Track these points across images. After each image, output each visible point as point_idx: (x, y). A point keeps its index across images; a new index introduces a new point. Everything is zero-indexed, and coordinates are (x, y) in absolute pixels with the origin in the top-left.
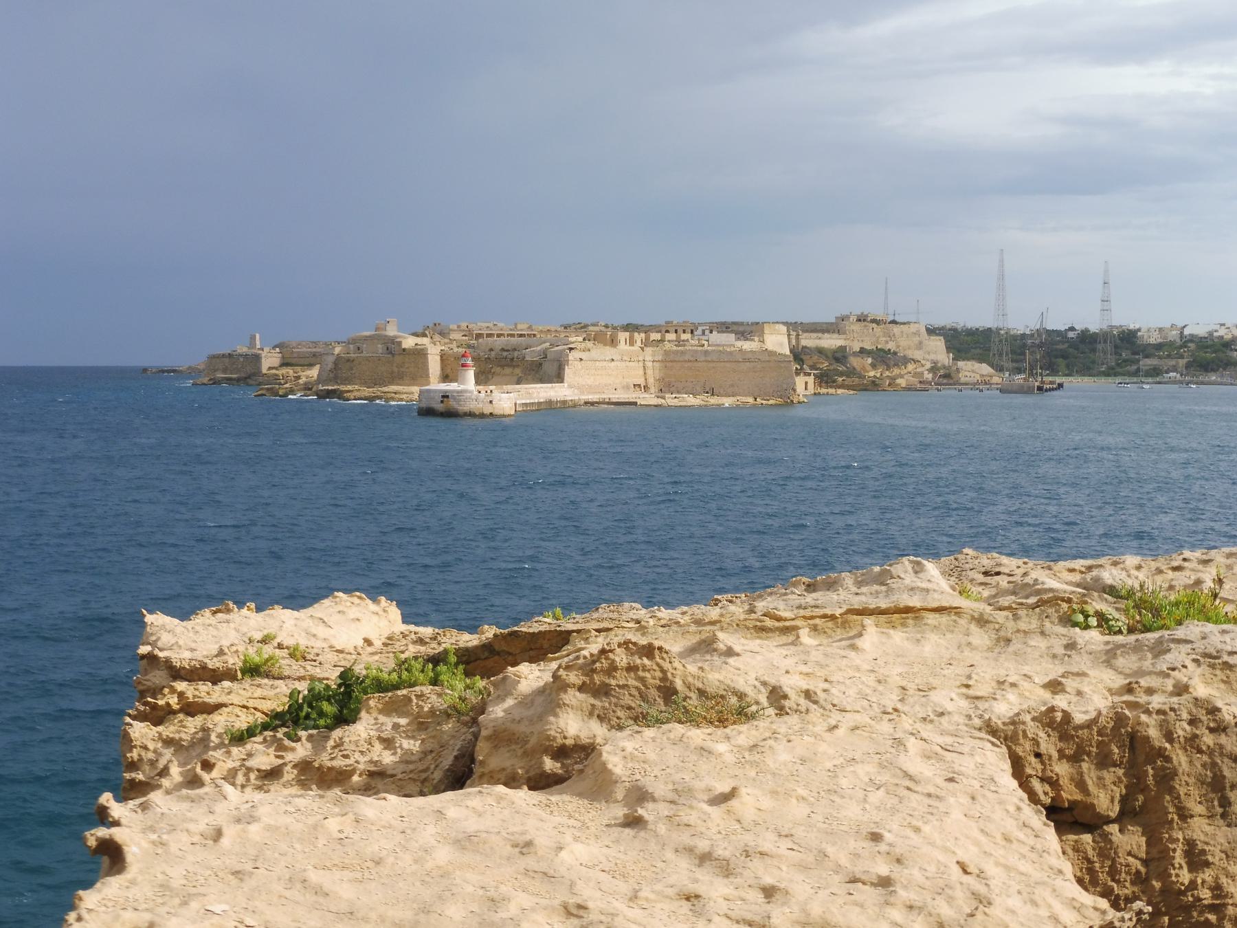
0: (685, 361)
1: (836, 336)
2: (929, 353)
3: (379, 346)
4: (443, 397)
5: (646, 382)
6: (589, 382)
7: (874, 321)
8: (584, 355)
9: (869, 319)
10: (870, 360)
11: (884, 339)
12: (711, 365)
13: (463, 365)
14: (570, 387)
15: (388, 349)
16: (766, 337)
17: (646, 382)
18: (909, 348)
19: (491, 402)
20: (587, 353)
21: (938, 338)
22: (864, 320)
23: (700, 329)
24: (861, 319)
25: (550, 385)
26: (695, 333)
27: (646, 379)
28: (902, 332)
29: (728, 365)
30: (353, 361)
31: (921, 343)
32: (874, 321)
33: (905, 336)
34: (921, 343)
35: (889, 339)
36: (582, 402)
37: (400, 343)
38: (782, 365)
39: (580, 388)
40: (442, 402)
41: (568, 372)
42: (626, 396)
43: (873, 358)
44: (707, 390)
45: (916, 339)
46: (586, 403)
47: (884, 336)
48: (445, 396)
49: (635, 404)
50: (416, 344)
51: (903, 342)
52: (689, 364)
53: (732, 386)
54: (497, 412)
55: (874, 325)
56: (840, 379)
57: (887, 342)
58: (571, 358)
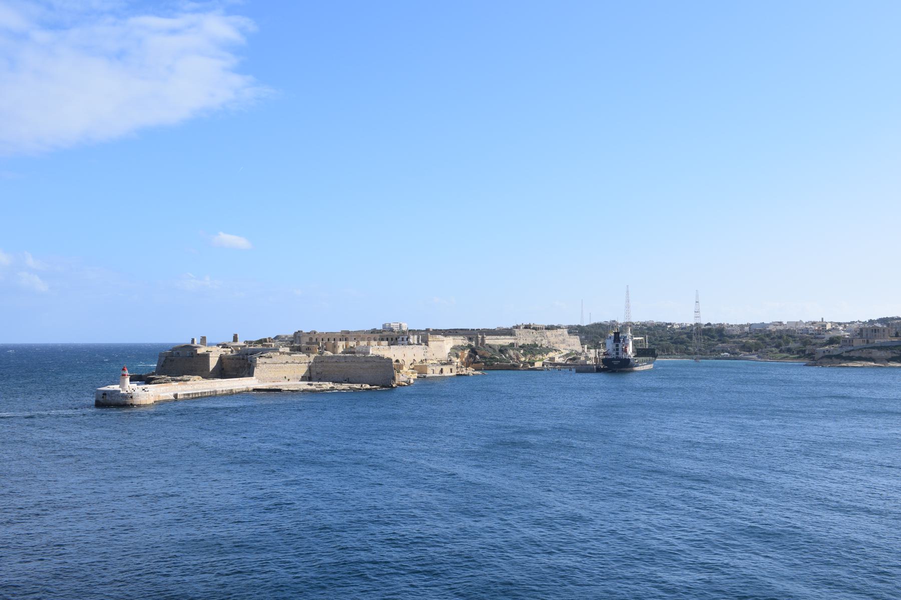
0: (333, 362)
1: (508, 337)
2: (569, 345)
4: (103, 394)
5: (310, 375)
6: (271, 376)
7: (534, 328)
8: (268, 361)
10: (522, 351)
11: (541, 338)
12: (348, 365)
13: (124, 375)
14: (257, 378)
15: (192, 354)
16: (429, 343)
17: (310, 375)
18: (556, 343)
19: (131, 397)
20: (270, 359)
21: (575, 337)
22: (530, 328)
23: (401, 337)
24: (527, 327)
25: (238, 379)
26: (398, 340)
27: (310, 373)
28: (552, 334)
29: (357, 365)
30: (173, 360)
31: (564, 340)
32: (534, 328)
34: (564, 340)
35: (543, 338)
36: (252, 389)
39: (263, 380)
40: (103, 397)
41: (256, 371)
42: (259, 386)
43: (524, 350)
44: (346, 379)
45: (561, 338)
46: (254, 390)
47: (541, 337)
49: (280, 390)
50: (207, 351)
51: (552, 339)
52: (336, 364)
53: (359, 377)
54: (135, 403)
55: (534, 331)
56: (496, 363)
57: (542, 340)
58: (258, 362)
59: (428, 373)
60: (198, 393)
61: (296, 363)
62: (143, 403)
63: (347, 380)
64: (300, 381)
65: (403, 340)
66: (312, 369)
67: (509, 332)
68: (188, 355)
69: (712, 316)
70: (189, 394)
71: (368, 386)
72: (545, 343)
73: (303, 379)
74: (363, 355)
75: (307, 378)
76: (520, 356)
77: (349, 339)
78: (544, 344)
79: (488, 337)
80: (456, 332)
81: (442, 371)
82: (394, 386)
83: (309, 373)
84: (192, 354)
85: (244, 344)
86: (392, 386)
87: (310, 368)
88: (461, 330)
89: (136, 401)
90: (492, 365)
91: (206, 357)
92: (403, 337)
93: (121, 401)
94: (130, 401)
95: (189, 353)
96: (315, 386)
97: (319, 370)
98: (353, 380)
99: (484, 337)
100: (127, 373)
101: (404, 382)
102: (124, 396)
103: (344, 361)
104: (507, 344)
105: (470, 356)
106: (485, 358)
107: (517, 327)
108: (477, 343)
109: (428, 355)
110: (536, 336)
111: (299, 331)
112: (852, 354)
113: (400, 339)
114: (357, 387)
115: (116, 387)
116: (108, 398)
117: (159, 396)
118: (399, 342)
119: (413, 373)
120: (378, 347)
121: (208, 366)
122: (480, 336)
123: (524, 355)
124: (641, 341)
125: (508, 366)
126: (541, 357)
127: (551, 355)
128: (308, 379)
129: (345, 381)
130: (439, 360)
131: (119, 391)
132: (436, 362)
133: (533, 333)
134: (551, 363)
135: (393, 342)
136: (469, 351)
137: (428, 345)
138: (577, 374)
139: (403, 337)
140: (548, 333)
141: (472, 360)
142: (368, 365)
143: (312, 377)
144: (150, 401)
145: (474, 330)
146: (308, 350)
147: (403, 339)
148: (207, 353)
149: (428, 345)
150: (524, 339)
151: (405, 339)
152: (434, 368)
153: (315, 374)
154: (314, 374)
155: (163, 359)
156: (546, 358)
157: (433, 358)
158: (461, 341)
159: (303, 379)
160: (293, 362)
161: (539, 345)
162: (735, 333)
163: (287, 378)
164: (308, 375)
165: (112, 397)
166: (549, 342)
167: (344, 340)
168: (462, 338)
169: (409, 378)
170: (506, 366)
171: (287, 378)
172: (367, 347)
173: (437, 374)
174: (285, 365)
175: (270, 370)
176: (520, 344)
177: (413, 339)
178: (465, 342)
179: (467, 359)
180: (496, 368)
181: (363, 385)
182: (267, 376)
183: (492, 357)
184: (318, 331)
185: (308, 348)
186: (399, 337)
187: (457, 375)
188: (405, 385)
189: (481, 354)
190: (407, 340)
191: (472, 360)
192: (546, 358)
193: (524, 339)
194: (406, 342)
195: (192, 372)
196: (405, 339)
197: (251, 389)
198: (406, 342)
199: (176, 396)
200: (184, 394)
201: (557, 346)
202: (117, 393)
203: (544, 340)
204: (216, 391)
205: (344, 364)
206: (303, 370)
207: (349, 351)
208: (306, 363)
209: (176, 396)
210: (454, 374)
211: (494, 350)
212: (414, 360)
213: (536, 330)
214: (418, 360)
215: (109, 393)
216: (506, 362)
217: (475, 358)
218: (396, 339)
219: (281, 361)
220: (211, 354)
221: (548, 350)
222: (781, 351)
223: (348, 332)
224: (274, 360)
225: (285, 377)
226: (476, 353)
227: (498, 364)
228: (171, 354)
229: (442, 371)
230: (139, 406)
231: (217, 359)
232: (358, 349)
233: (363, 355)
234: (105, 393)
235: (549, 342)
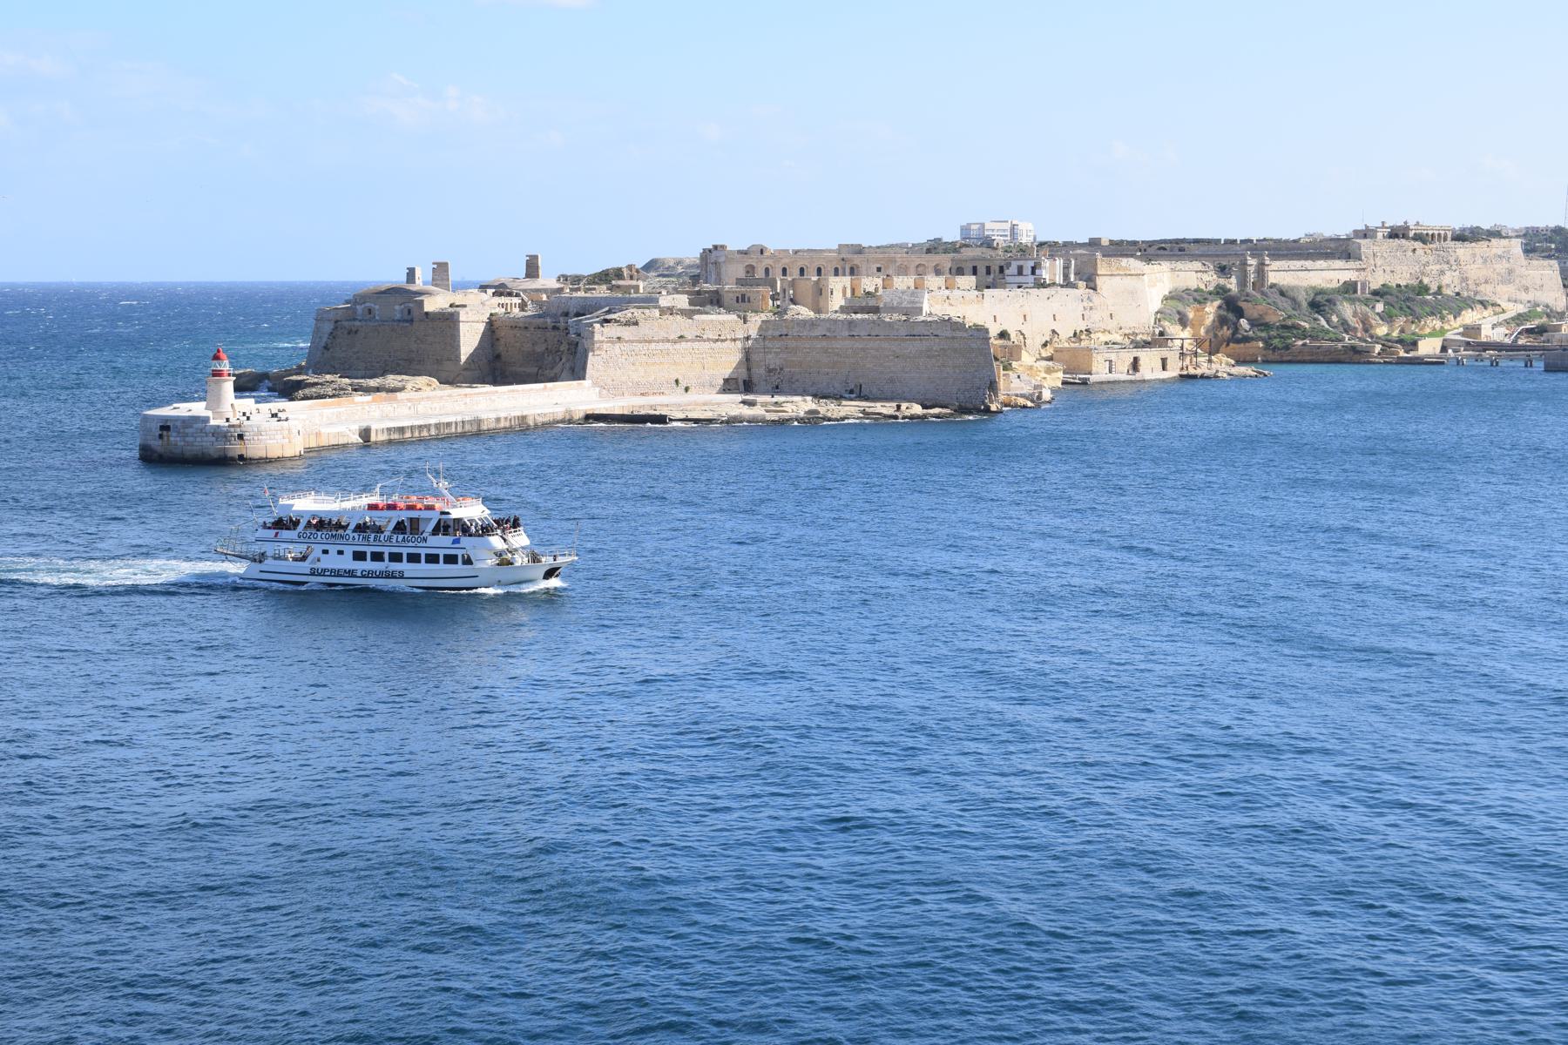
1: (1339, 263)
2: (1526, 289)
3: (397, 307)
7: (1419, 238)
8: (626, 332)
9: (1411, 234)
10: (1380, 307)
11: (1438, 267)
12: (858, 345)
13: (217, 374)
15: (409, 312)
16: (1099, 281)
18: (1486, 282)
19: (241, 437)
20: (633, 328)
21: (1546, 262)
22: (1405, 236)
24: (1396, 234)
25: (541, 385)
26: (1007, 272)
27: (749, 369)
29: (885, 345)
31: (1510, 272)
32: (1419, 238)
33: (1480, 261)
34: (1510, 272)
35: (1446, 267)
36: (582, 415)
37: (421, 303)
38: (974, 346)
40: (161, 436)
41: (593, 361)
45: (1501, 267)
46: (590, 417)
48: (165, 428)
49: (661, 419)
50: (451, 306)
51: (1475, 271)
52: (824, 344)
53: (892, 381)
55: (1418, 245)
56: (1300, 343)
57: (1442, 272)
58: (597, 337)
59: (1094, 369)
60: (428, 427)
61: (709, 340)
62: (274, 453)
63: (857, 390)
64: (719, 392)
65: (1020, 271)
66: (754, 357)
67: (1340, 249)
68: (398, 316)
70: (402, 430)
71: (917, 409)
72: (1450, 282)
73: (729, 386)
74: (904, 318)
75: (741, 383)
76: (1374, 320)
77: (863, 269)
78: (1448, 286)
79: (1276, 264)
80: (1181, 250)
81: (1135, 365)
82: (993, 408)
83: (743, 371)
84: (409, 312)
85: (558, 286)
86: (987, 410)
87: (748, 354)
88: (1196, 241)
89: (254, 449)
90: (1287, 348)
91: (448, 321)
92: (1021, 263)
93: (213, 447)
94: (236, 449)
95: (402, 311)
96: (763, 406)
97: (773, 360)
98: (875, 391)
99: (1263, 264)
100: (225, 366)
101: (1022, 396)
102: (219, 433)
103: (847, 334)
104: (1335, 285)
105: (1221, 321)
106: (1266, 326)
107: (1367, 234)
108: (1242, 283)
109: (1096, 319)
110: (1424, 259)
111: (716, 247)
113: (1013, 269)
114: (885, 411)
115: (197, 409)
116: (173, 438)
117: (318, 434)
118: (1009, 279)
119: (1049, 371)
120: (947, 292)
121: (458, 348)
122: (1252, 262)
123: (1387, 317)
125: (1336, 350)
126: (1438, 324)
127: (1469, 317)
128: (742, 387)
129: (851, 392)
130: (1127, 332)
131: (206, 420)
132: (1117, 338)
133: (1414, 250)
134: (1468, 343)
135: (990, 279)
136: (1220, 307)
137: (1094, 289)
138: (1551, 377)
139: (1021, 263)
140: (1463, 251)
141: (1226, 332)
142: (914, 347)
143: (755, 380)
144: (295, 447)
145: (1234, 242)
146: (743, 300)
147: (1020, 271)
148: (450, 310)
149: (1094, 289)
150: (1388, 269)
151: (1027, 271)
152: (1113, 357)
153: (762, 371)
154: (759, 372)
155: (328, 327)
156: (1454, 327)
157: (1111, 325)
158: (1194, 275)
159: (729, 386)
160: (699, 338)
161: (1434, 288)
163: (683, 384)
164: (743, 374)
165: (187, 435)
166: (1464, 280)
167: (848, 271)
168: (1197, 265)
169: (1039, 387)
170: (1329, 351)
171: (683, 384)
172: (913, 294)
173: (1121, 373)
174: (677, 346)
175: (632, 359)
176: (1375, 286)
177: (1052, 269)
178: (1206, 277)
179: (1213, 329)
180: (1299, 358)
181: (904, 406)
182: (624, 379)
183: (1289, 323)
184: (772, 246)
185: (743, 296)
186: (1009, 265)
187: (1181, 376)
188: (1025, 407)
189: (1255, 315)
190: (1033, 273)
191: (1226, 332)
192: (1454, 327)
194: (1031, 279)
195: (411, 365)
196: (1027, 271)
197: (579, 415)
198: (1031, 279)
199: (365, 433)
200: (389, 430)
201: (1486, 292)
202: (200, 425)
203: (1448, 273)
204: (479, 421)
205: (848, 343)
206: (728, 360)
207: (864, 304)
208: (735, 340)
209: (365, 433)
210: (1173, 372)
211: (1295, 303)
212: (1054, 331)
213: (1424, 242)
214: (1065, 332)
215: (178, 424)
216: (1330, 340)
217: (1236, 328)
218: (1001, 270)
219: (663, 334)
220: (462, 312)
221: (1460, 303)
223: (859, 250)
224: (644, 329)
225: (677, 381)
226: (1240, 313)
227: (1304, 345)
228: (350, 314)
229: (1135, 365)
230: (267, 461)
231: (481, 327)
232: (888, 300)
233: (904, 318)
234: (165, 426)
235: (1464, 280)
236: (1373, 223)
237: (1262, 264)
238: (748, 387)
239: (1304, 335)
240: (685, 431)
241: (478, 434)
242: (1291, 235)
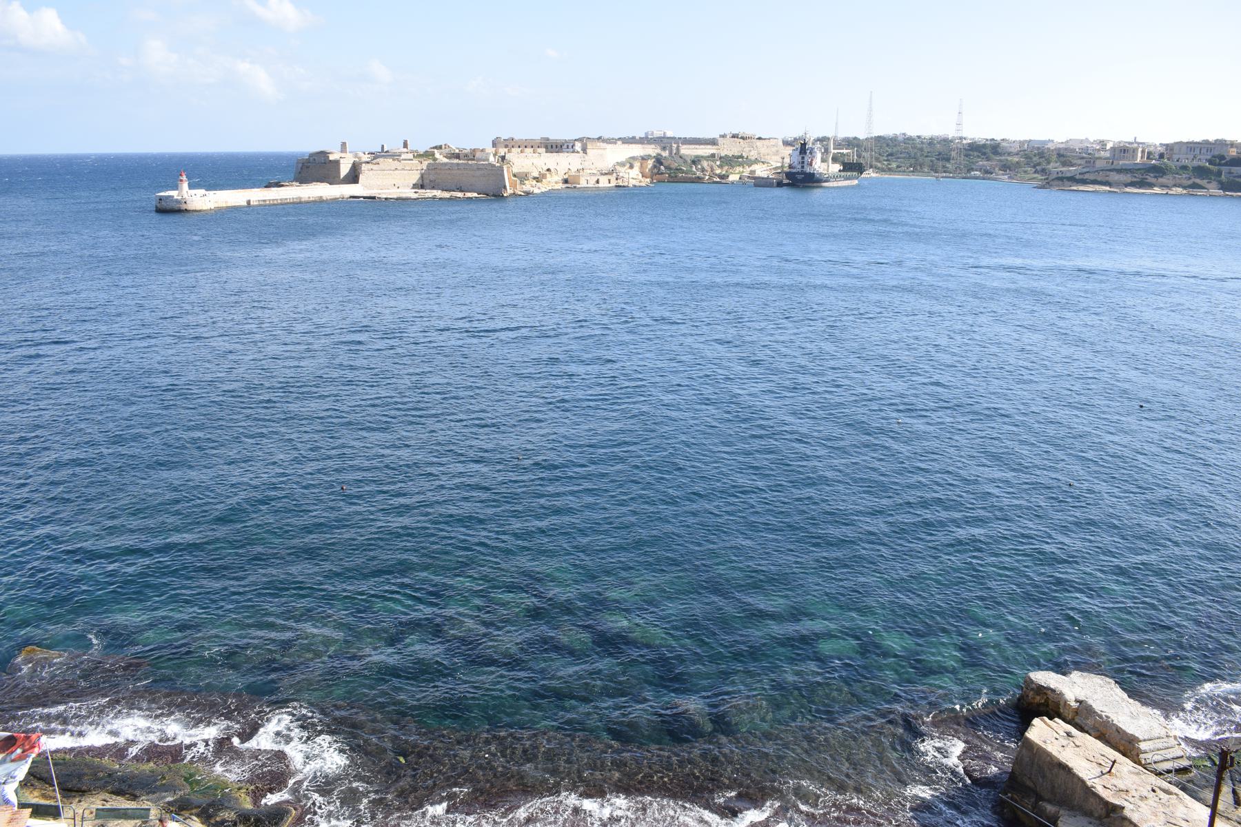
1: (709, 147)
7: (743, 138)
24: (734, 136)
32: (743, 138)
45: (774, 149)
51: (763, 151)
62: (198, 208)
67: (713, 142)
69: (977, 130)
70: (265, 201)
71: (475, 195)
72: (753, 155)
73: (415, 186)
75: (421, 185)
76: (715, 167)
79: (685, 146)
81: (598, 182)
87: (422, 176)
89: (190, 207)
91: (337, 163)
93: (176, 206)
97: (432, 177)
100: (184, 178)
102: (178, 201)
105: (655, 167)
106: (670, 169)
107: (723, 136)
108: (671, 153)
109: (586, 165)
112: (1086, 176)
115: (174, 193)
121: (339, 173)
122: (675, 146)
123: (721, 167)
124: (848, 155)
126: (741, 169)
127: (754, 167)
140: (759, 143)
141: (656, 171)
142: (478, 173)
154: (426, 182)
155: (300, 165)
156: (746, 171)
157: (592, 167)
158: (652, 150)
160: (403, 169)
162: (1012, 150)
164: (420, 182)
168: (653, 146)
170: (690, 178)
173: (592, 184)
177: (578, 146)
179: (651, 170)
191: (656, 171)
192: (746, 171)
193: (728, 149)
195: (321, 180)
199: (249, 202)
201: (768, 158)
204: (300, 198)
206: (415, 177)
209: (249, 202)
210: (613, 184)
211: (685, 161)
214: (574, 169)
217: (659, 169)
221: (751, 163)
222: (1036, 172)
224: (382, 166)
226: (661, 164)
228: (308, 161)
229: (598, 182)
230: (196, 211)
236: (727, 132)
237: (678, 147)
238: (422, 187)
239: (683, 172)
240: (365, 202)
241: (300, 203)
242: (688, 136)
